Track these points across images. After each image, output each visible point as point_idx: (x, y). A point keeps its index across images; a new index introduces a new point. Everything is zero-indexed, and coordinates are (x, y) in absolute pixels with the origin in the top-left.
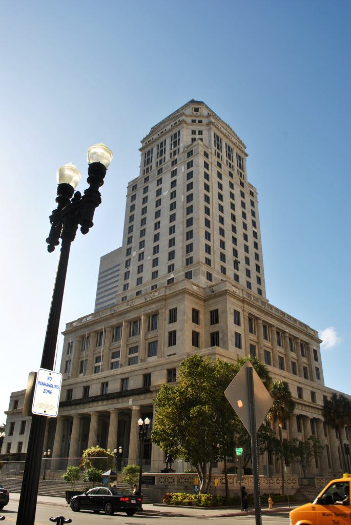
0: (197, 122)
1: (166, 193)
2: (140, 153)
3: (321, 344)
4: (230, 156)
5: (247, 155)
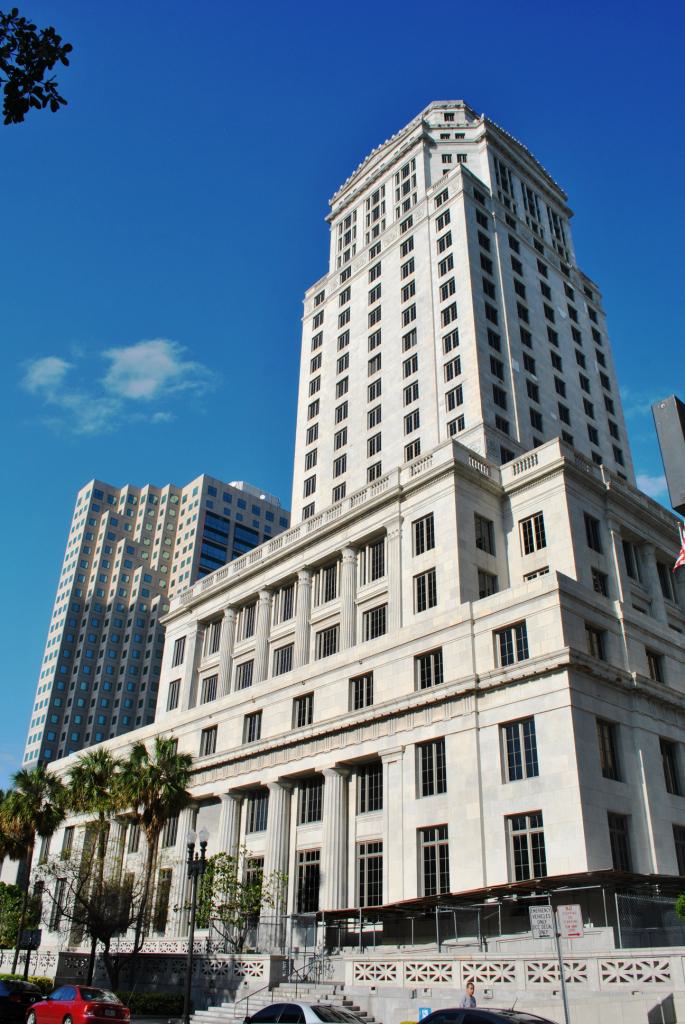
0: (453, 137)
4: (532, 209)
5: (570, 214)
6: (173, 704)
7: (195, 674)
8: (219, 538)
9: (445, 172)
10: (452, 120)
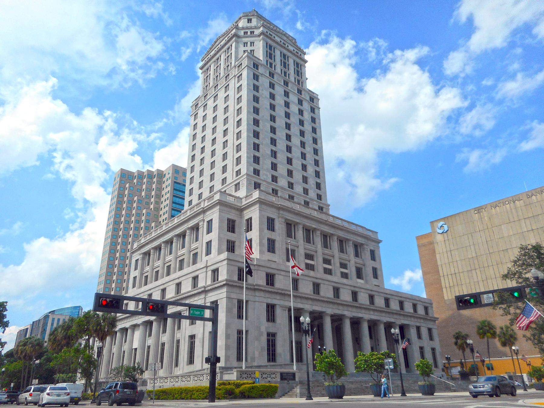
0: (249, 33)
1: (221, 110)
3: (380, 245)
4: (285, 65)
6: (134, 286)
7: (142, 274)
8: (181, 194)
9: (244, 51)
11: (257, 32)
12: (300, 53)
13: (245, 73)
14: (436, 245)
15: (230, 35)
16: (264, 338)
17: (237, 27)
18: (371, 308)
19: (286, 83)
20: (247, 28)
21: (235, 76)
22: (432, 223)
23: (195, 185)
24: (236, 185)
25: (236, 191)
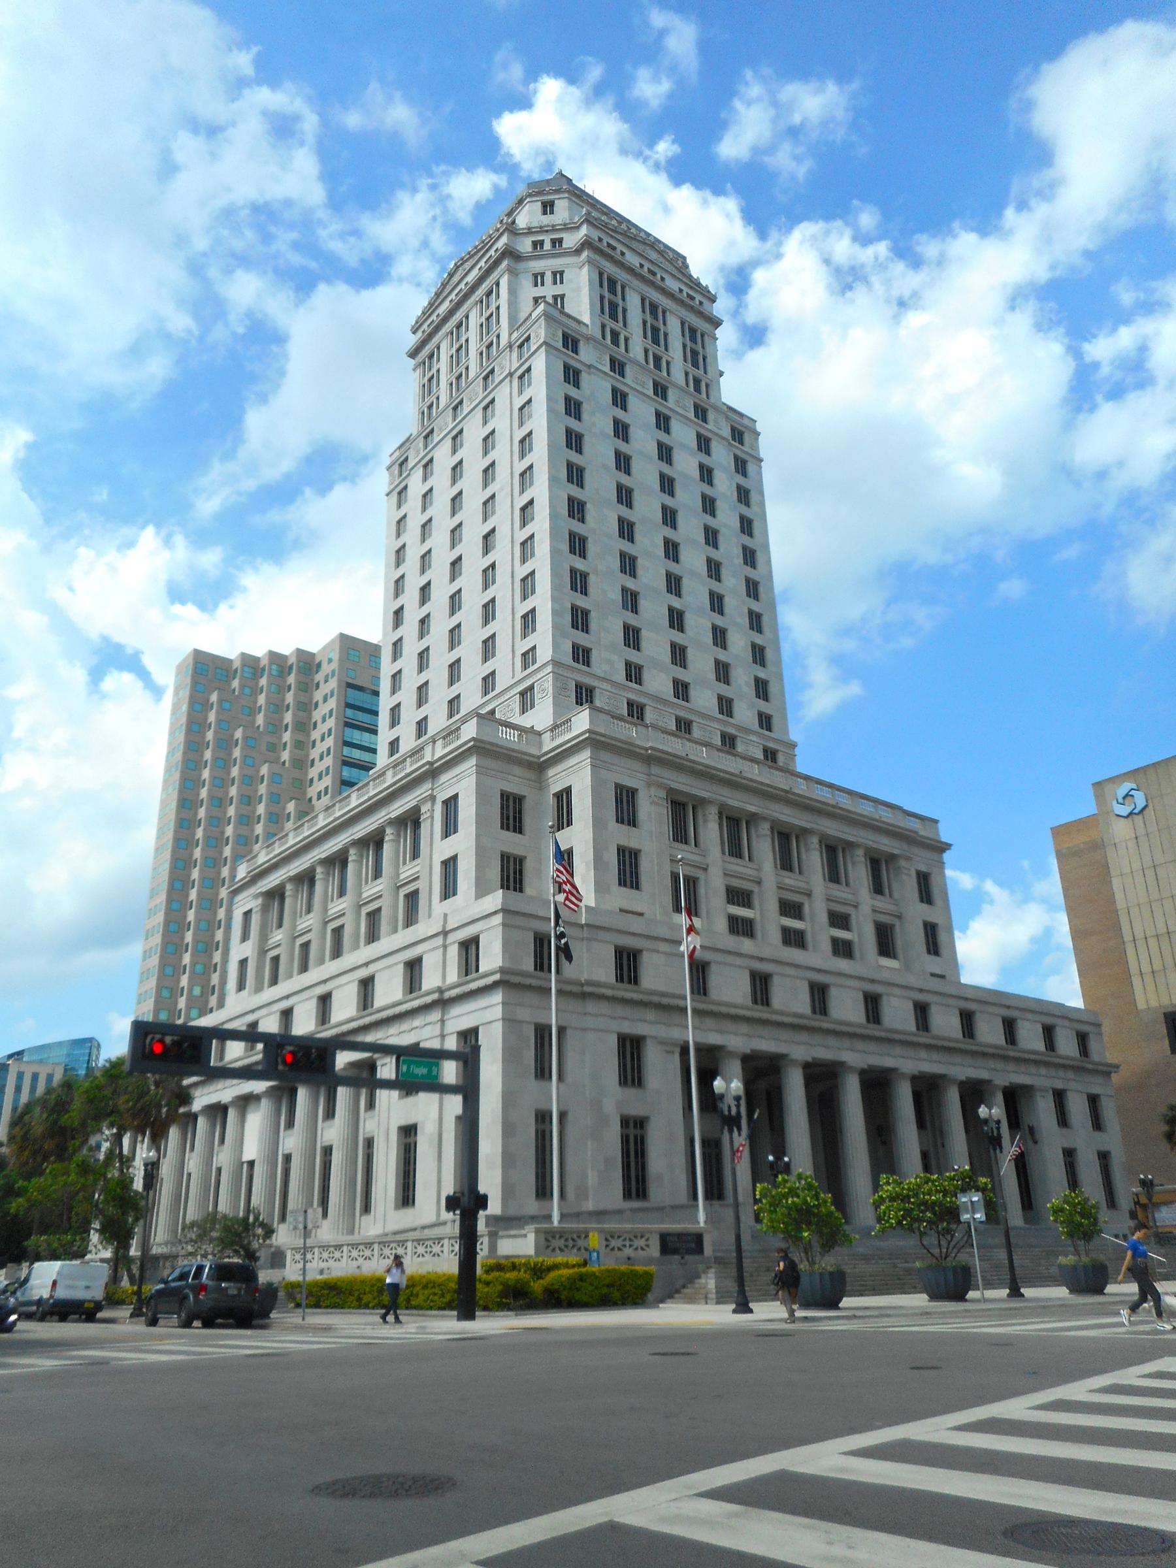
0: (547, 246)
2: (412, 362)
3: (947, 856)
4: (655, 335)
6: (241, 986)
7: (262, 951)
10: (552, 212)
11: (571, 240)
12: (698, 298)
13: (539, 364)
14: (1110, 852)
15: (492, 252)
16: (614, 1133)
17: (511, 229)
18: (922, 1040)
19: (661, 390)
20: (542, 230)
21: (511, 375)
22: (1098, 786)
23: (407, 696)
24: (523, 694)
25: (523, 711)
